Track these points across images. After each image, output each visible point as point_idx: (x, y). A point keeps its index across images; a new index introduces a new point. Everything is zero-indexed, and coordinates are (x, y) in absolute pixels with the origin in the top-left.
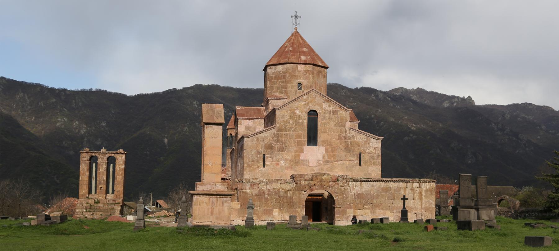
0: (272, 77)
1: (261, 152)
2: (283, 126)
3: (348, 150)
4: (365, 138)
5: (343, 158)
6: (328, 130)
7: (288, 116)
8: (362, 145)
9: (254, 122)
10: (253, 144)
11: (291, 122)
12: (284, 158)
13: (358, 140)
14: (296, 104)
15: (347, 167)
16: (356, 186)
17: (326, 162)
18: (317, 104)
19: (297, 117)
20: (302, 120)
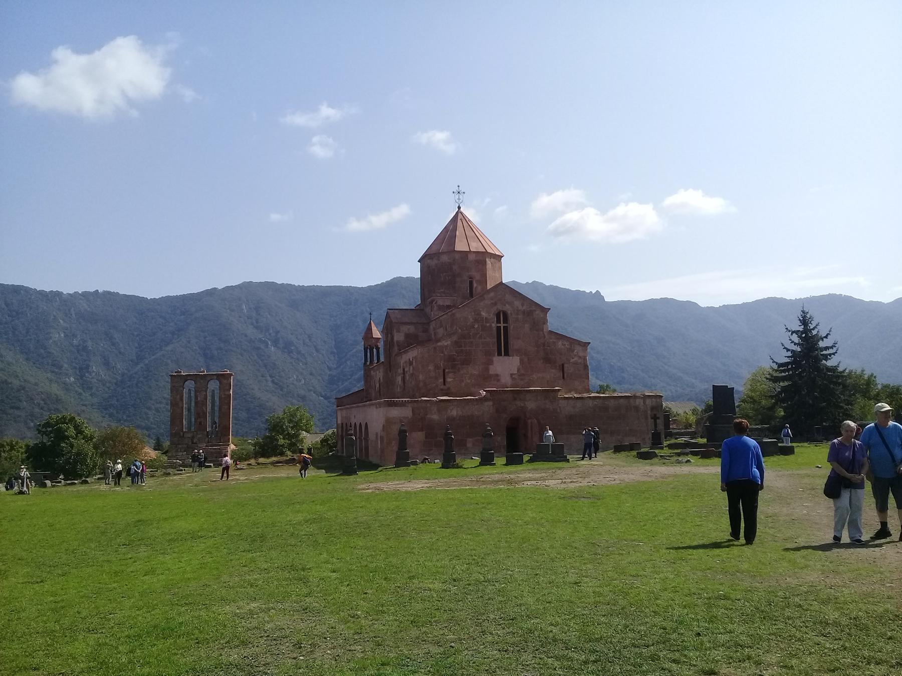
3: (547, 360)
7: (471, 319)
11: (476, 326)
13: (559, 346)
14: (482, 304)
15: (548, 381)
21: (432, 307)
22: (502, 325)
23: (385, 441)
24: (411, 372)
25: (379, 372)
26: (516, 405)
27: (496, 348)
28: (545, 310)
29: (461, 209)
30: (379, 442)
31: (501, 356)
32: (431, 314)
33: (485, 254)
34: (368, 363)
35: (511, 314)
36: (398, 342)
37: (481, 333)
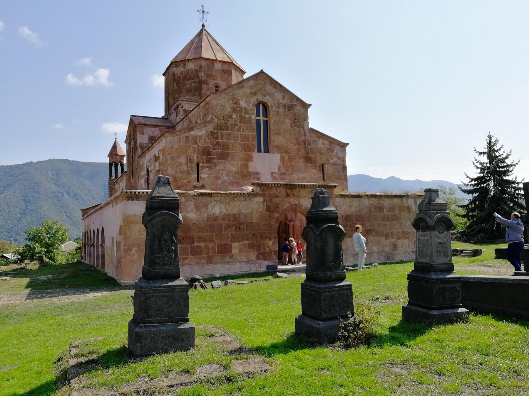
0: (179, 77)
1: (194, 159)
2: (224, 122)
3: (308, 159)
4: (328, 144)
6: (283, 131)
7: (229, 108)
9: (160, 130)
10: (181, 145)
11: (234, 116)
12: (227, 169)
14: (241, 91)
16: (343, 203)
17: (282, 175)
18: (268, 95)
19: (242, 111)
20: (249, 116)
21: (177, 112)
22: (262, 118)
23: (122, 248)
24: (157, 168)
26: (289, 203)
27: (255, 143)
28: (306, 106)
29: (205, 28)
30: (115, 248)
31: (261, 152)
32: (176, 119)
33: (232, 63)
34: (113, 178)
35: (272, 106)
36: (141, 144)
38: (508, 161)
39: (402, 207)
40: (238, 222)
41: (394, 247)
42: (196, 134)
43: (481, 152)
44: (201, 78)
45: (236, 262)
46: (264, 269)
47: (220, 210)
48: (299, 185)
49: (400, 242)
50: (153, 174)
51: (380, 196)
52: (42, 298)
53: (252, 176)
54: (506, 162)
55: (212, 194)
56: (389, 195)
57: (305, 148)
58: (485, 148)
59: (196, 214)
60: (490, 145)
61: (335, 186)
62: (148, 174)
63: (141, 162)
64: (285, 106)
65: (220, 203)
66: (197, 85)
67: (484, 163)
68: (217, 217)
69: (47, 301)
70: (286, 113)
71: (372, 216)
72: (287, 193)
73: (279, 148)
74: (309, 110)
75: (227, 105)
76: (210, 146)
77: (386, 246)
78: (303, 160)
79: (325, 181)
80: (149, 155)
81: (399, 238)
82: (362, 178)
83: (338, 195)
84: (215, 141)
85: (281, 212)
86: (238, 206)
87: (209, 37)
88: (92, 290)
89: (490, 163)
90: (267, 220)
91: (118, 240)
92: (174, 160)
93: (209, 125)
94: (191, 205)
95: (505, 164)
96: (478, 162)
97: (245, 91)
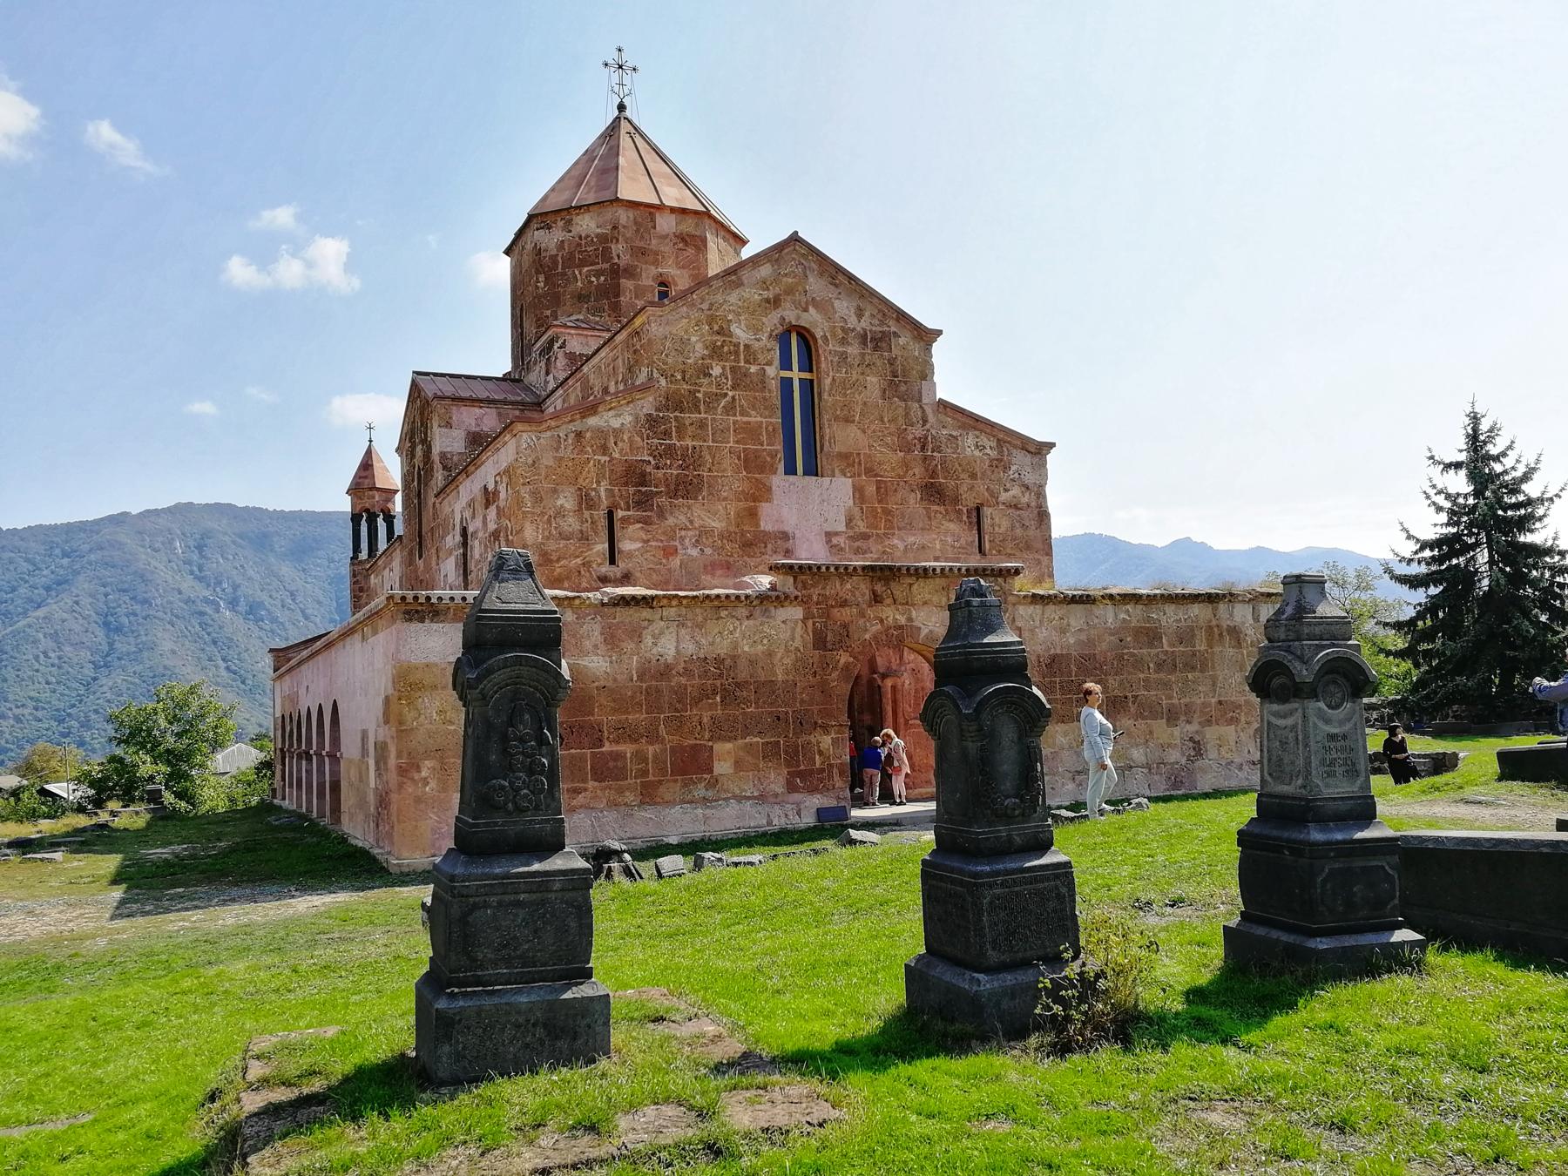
0: (554, 258)
3: (934, 492)
5: (920, 526)
8: (983, 474)
9: (499, 415)
14: (733, 297)
19: (737, 353)
20: (758, 367)
22: (796, 375)
23: (392, 761)
24: (492, 526)
25: (391, 570)
26: (882, 621)
27: (779, 447)
28: (926, 336)
29: (628, 113)
30: (372, 762)
32: (546, 382)
33: (705, 215)
34: (364, 555)
35: (825, 338)
36: (443, 455)
37: (730, 393)
38: (1531, 489)
39: (1216, 629)
40: (731, 680)
41: (1194, 749)
42: (602, 423)
43: (1447, 461)
44: (617, 261)
45: (725, 799)
46: (809, 820)
47: (677, 648)
48: (908, 569)
49: (1211, 733)
50: (480, 543)
51: (1151, 599)
52: (160, 913)
53: (769, 546)
54: (1524, 492)
55: (653, 598)
56: (1177, 595)
57: (925, 459)
58: (1461, 451)
59: (608, 659)
60: (1475, 440)
61: (1017, 572)
62: (465, 544)
63: (446, 509)
64: (863, 338)
65: (677, 626)
66: (606, 280)
67: (1458, 495)
68: (668, 667)
69: (174, 921)
70: (867, 357)
71: (1126, 657)
72: (874, 593)
73: (848, 461)
74: (936, 348)
75: (694, 339)
76: (646, 458)
77: (1169, 745)
78: (919, 496)
79: (985, 554)
80: (469, 488)
81: (1209, 722)
82: (1098, 546)
83: (1025, 597)
84: (661, 444)
85: (856, 650)
86: (731, 632)
87: (638, 139)
88: (306, 889)
89: (1478, 493)
90: (815, 673)
91: (381, 738)
92: (541, 501)
93: (643, 398)
94: (593, 630)
95: (1521, 498)
96: (1439, 492)
97: (746, 295)
